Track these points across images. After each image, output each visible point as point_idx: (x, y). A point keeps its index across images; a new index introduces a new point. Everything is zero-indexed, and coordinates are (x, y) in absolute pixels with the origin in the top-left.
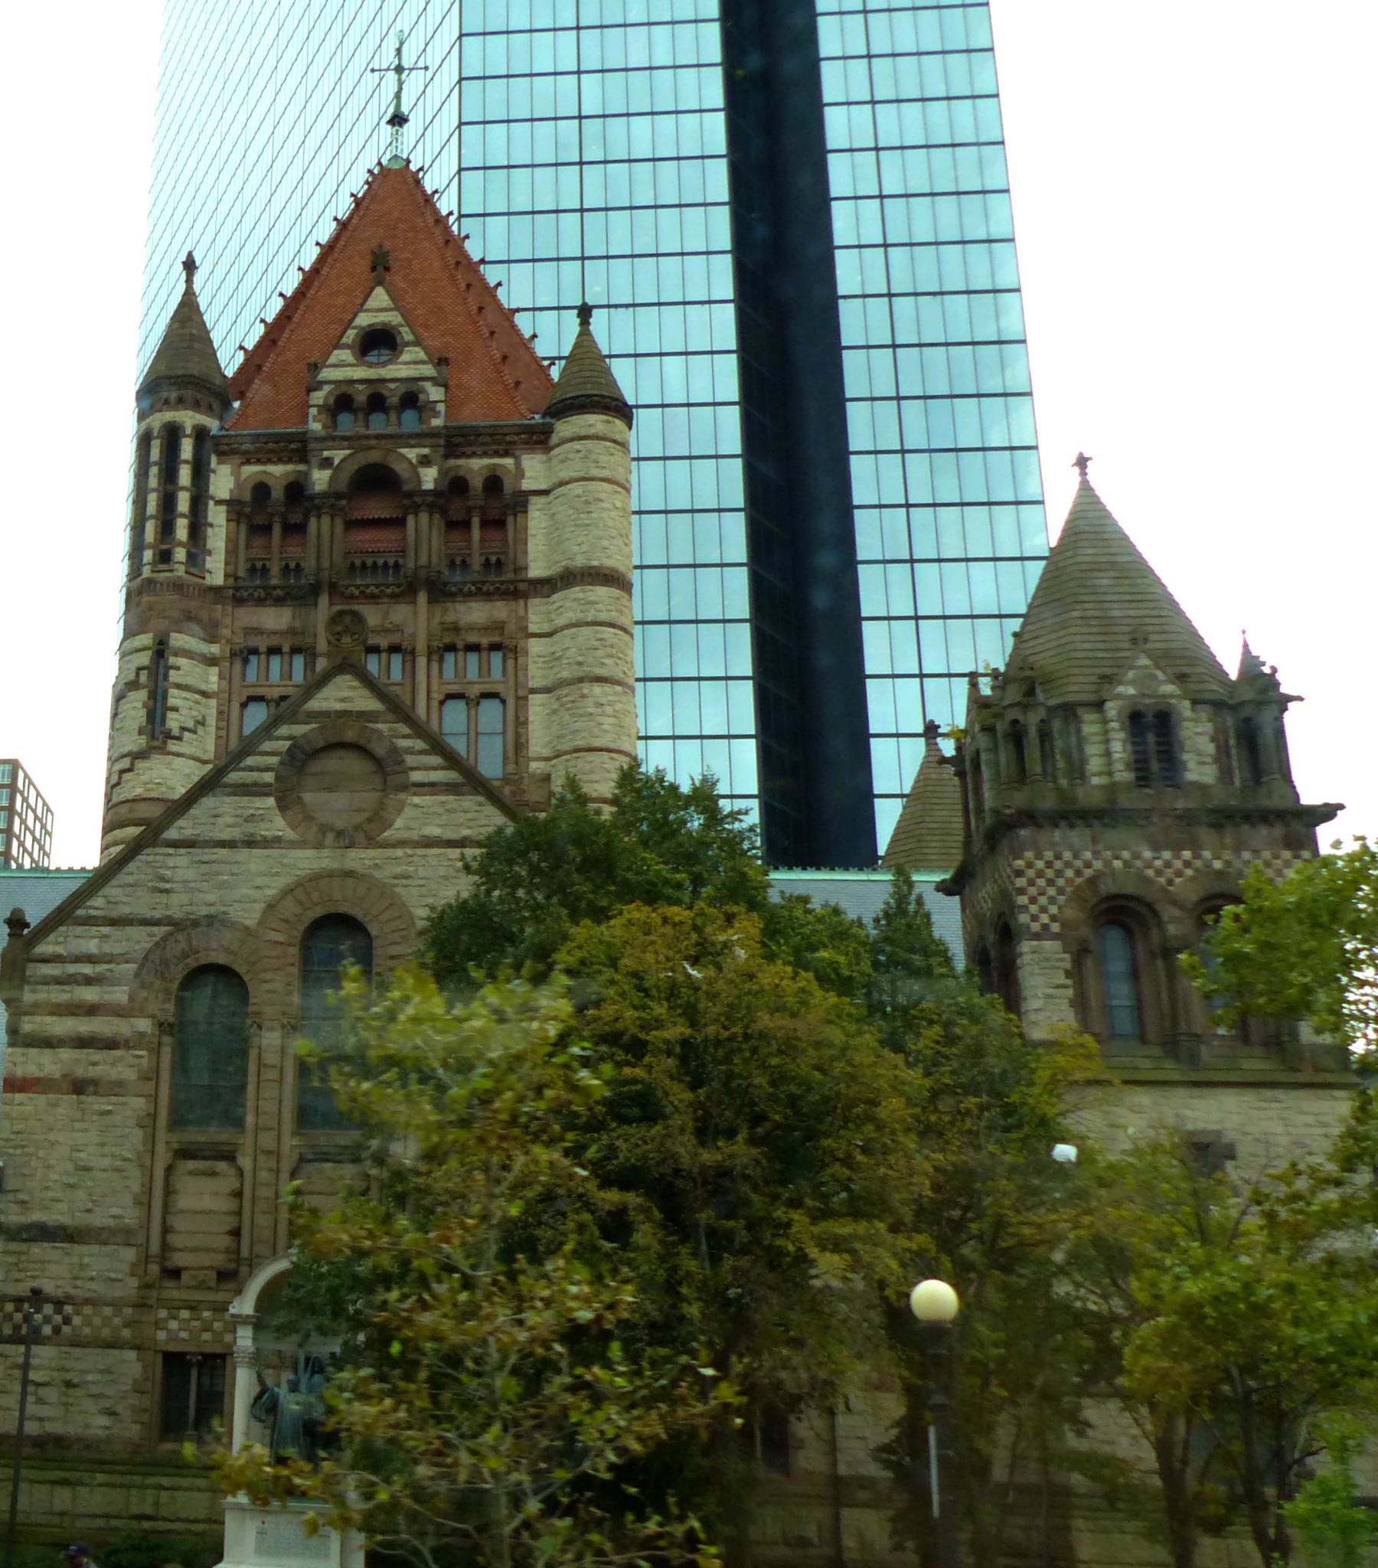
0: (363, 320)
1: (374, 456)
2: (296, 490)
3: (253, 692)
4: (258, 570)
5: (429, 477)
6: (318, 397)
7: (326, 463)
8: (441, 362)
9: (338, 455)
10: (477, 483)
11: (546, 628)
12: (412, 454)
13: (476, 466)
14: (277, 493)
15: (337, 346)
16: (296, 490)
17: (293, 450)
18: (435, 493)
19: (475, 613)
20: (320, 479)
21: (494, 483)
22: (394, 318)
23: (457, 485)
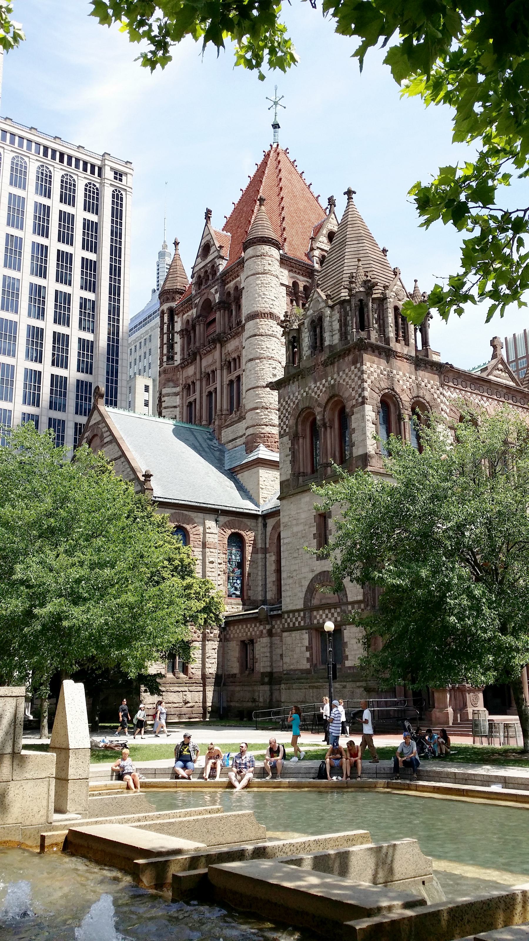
6: (317, 253)
14: (301, 289)
17: (308, 272)
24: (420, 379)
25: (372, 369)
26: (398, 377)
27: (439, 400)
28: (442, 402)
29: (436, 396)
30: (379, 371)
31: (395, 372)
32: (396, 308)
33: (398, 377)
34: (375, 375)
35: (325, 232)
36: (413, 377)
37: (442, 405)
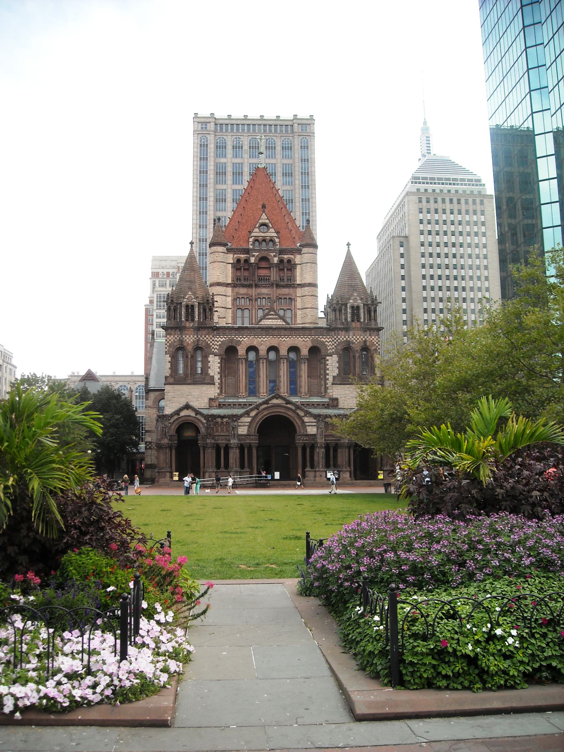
0: (261, 221)
1: (264, 254)
2: (247, 261)
3: (239, 307)
4: (238, 279)
5: (276, 260)
6: (251, 240)
7: (254, 256)
8: (278, 233)
9: (256, 254)
10: (285, 261)
11: (300, 295)
12: (272, 254)
13: (286, 256)
14: (242, 262)
15: (255, 228)
16: (247, 261)
18: (277, 264)
19: (285, 291)
20: (252, 260)
21: (289, 261)
22: (267, 221)
23: (281, 261)
24: (199, 336)
25: (170, 338)
26: (186, 338)
27: (211, 344)
28: (213, 344)
29: (209, 342)
30: (174, 338)
31: (184, 336)
32: (187, 306)
33: (186, 338)
34: (172, 340)
35: (257, 226)
36: (195, 336)
37: (213, 346)
